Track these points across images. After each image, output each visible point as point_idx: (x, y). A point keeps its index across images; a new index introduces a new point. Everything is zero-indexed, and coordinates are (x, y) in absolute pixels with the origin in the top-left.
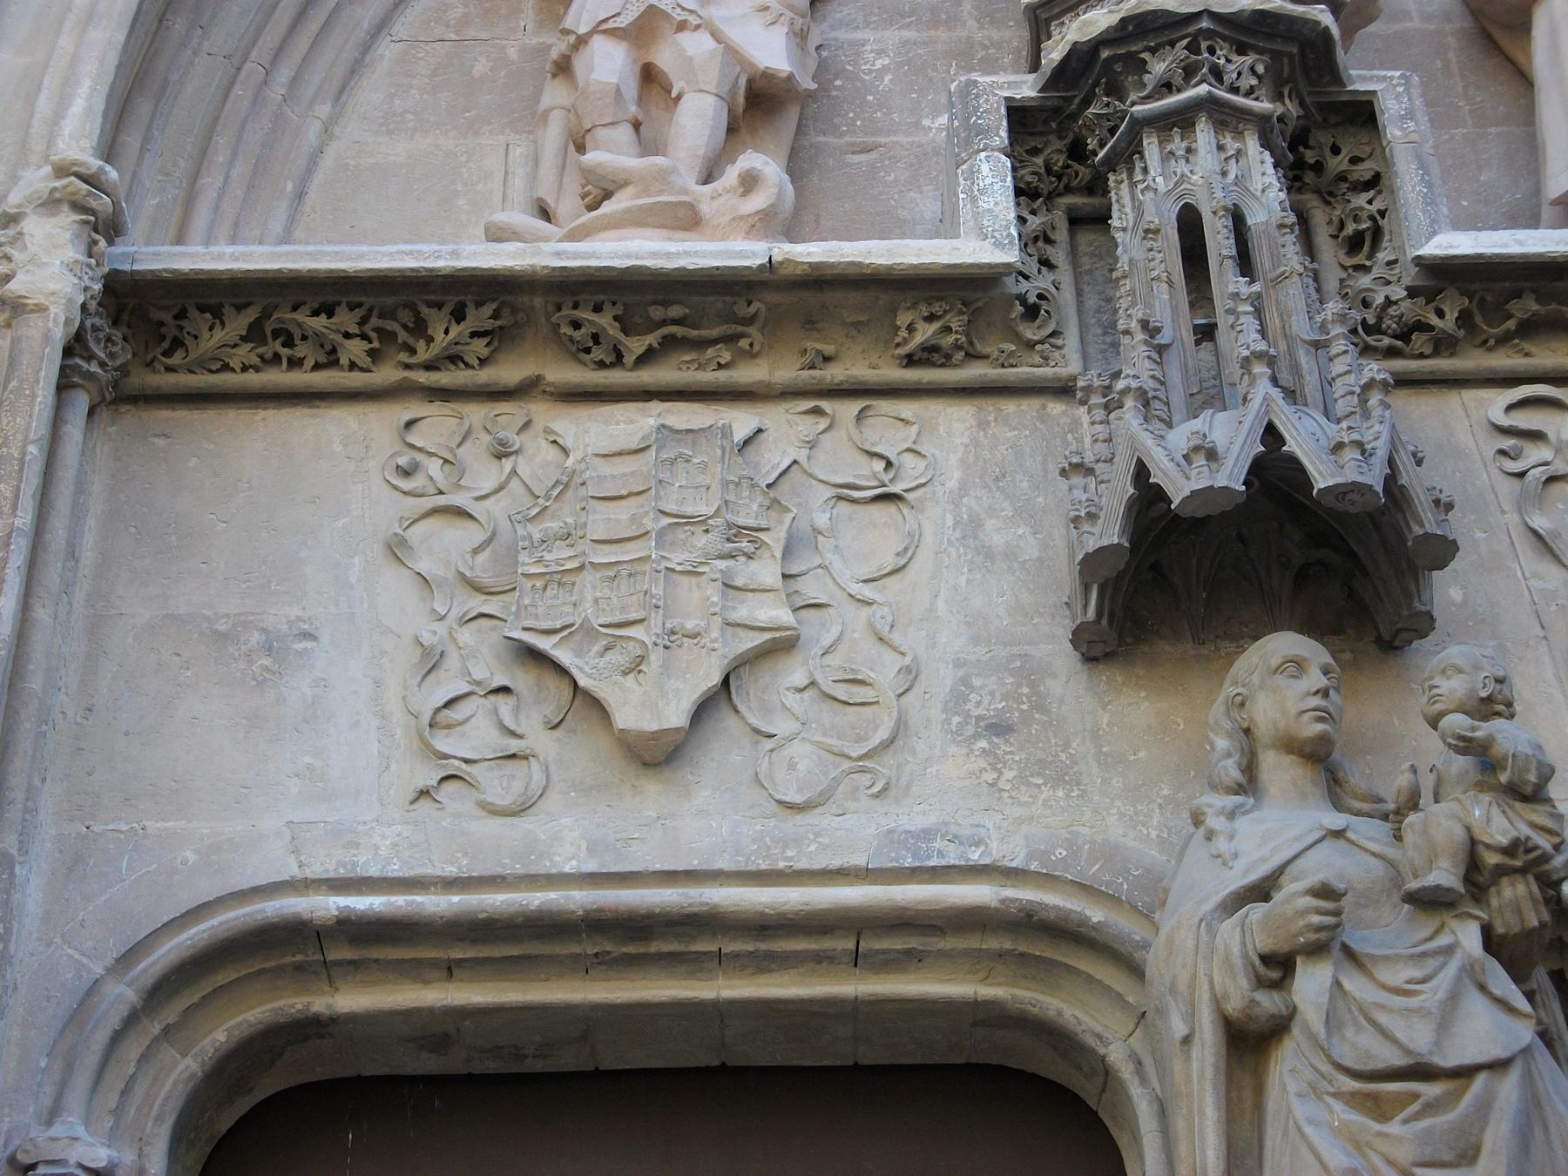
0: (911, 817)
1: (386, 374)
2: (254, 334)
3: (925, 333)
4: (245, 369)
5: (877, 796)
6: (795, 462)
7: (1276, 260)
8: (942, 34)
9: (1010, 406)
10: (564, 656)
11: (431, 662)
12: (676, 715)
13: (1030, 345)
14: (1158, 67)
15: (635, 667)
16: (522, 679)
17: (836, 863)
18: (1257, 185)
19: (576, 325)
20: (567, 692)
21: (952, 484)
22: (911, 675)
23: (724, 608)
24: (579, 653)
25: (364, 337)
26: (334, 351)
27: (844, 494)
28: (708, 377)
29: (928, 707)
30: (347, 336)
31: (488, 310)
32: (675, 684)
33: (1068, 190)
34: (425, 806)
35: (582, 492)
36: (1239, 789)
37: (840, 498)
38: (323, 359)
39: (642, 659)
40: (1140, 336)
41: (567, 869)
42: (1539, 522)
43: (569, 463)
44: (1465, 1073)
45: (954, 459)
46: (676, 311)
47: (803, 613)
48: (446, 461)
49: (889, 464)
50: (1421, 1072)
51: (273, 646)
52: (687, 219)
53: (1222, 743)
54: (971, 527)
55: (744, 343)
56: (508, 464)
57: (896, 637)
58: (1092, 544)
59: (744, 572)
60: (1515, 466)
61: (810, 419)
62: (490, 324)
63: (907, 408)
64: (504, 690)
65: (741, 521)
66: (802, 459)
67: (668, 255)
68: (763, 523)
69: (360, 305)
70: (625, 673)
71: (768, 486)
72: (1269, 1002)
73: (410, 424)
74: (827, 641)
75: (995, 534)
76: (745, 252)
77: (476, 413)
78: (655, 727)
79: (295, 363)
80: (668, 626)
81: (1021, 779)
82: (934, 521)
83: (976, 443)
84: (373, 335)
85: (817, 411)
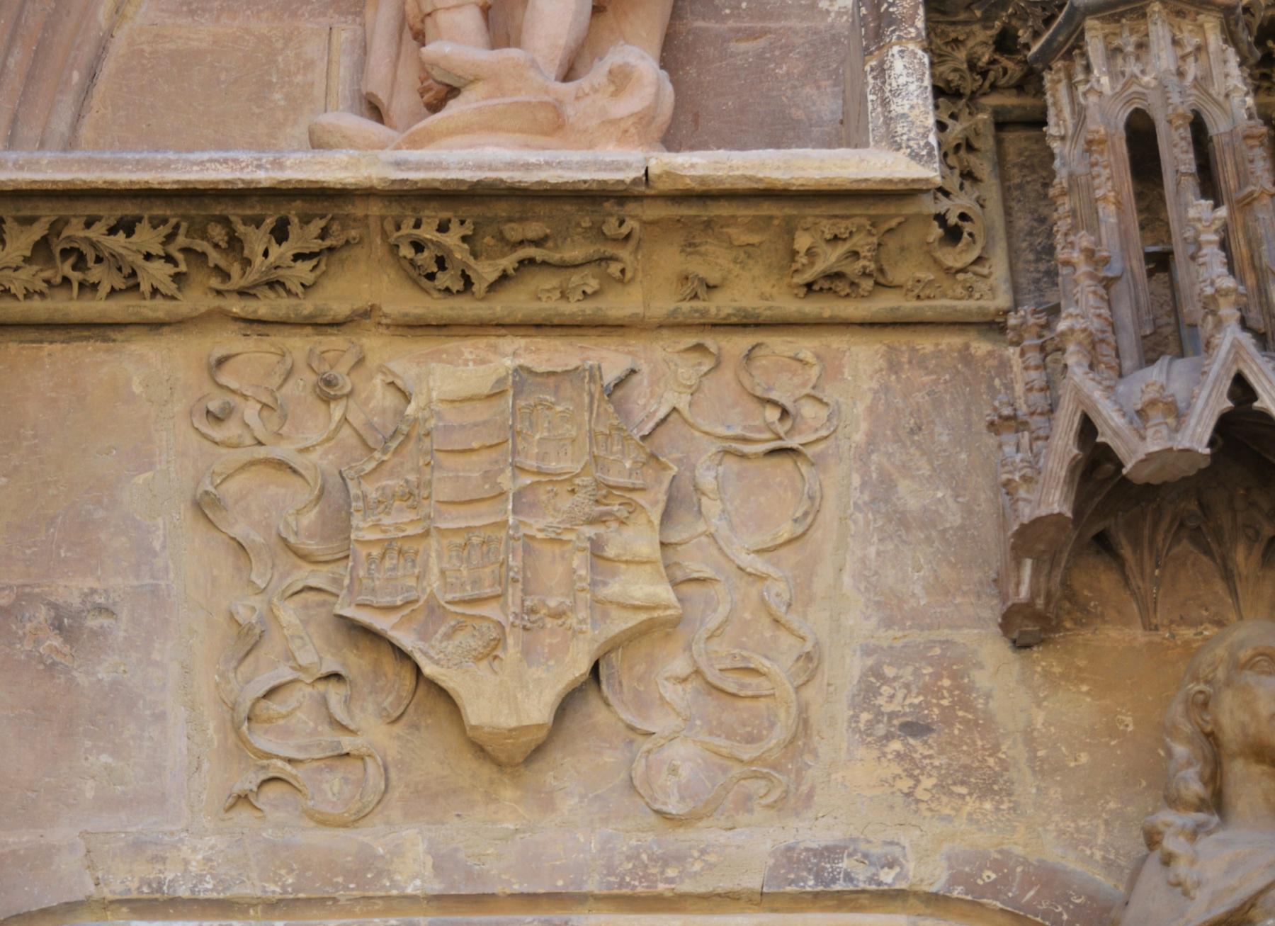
0: (811, 833)
1: (194, 300)
3: (830, 258)
4: (28, 295)
5: (768, 806)
6: (674, 409)
7: (1243, 177)
9: (926, 343)
10: (406, 640)
11: (248, 641)
12: (538, 710)
13: (952, 272)
15: (491, 652)
16: (355, 662)
17: (725, 885)
18: (1217, 90)
19: (418, 246)
20: (408, 680)
21: (859, 437)
22: (810, 661)
23: (594, 584)
24: (424, 636)
25: (169, 259)
26: (134, 274)
27: (731, 451)
28: (572, 308)
29: (833, 704)
30: (148, 257)
31: (315, 227)
32: (536, 672)
33: (994, 87)
34: (243, 815)
35: (427, 443)
36: (1201, 805)
37: (727, 452)
38: (120, 284)
39: (500, 642)
40: (1083, 268)
41: (409, 890)
43: (410, 410)
45: (860, 408)
46: (534, 229)
47: (685, 589)
48: (265, 405)
49: (785, 413)
52: (554, 124)
53: (1180, 750)
55: (614, 269)
56: (337, 411)
57: (793, 619)
58: (1027, 513)
59: (619, 541)
61: (694, 357)
62: (316, 245)
63: (806, 346)
64: (335, 676)
65: (612, 479)
66: (683, 404)
67: (527, 167)
68: (639, 483)
69: (164, 221)
70: (478, 659)
71: (644, 438)
73: (221, 362)
74: (713, 622)
75: (910, 496)
76: (617, 160)
78: (513, 723)
79: (88, 288)
80: (528, 603)
81: (942, 787)
82: (840, 483)
83: (886, 389)
84: (179, 257)
85: (699, 348)
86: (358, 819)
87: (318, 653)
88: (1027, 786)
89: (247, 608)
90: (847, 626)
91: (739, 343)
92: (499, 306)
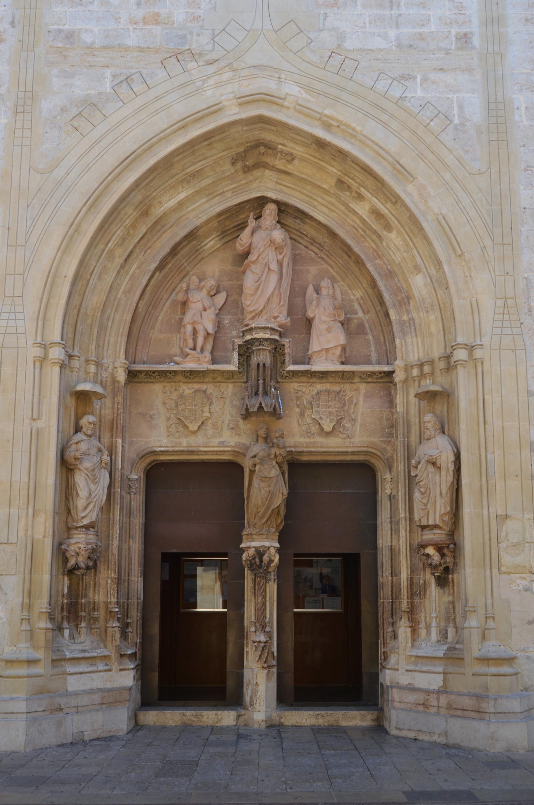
0: (222, 440)
2: (146, 375)
3: (227, 376)
8: (236, 317)
12: (196, 428)
14: (256, 344)
22: (223, 421)
42: (298, 403)
44: (271, 478)
50: (266, 477)
51: (151, 417)
54: (232, 402)
60: (297, 395)
72: (253, 469)
75: (235, 403)
77: (173, 384)
86: (179, 438)
87: (175, 421)
88: (243, 435)
89: (168, 415)
90: (227, 417)
91: (218, 384)
92: (193, 381)
